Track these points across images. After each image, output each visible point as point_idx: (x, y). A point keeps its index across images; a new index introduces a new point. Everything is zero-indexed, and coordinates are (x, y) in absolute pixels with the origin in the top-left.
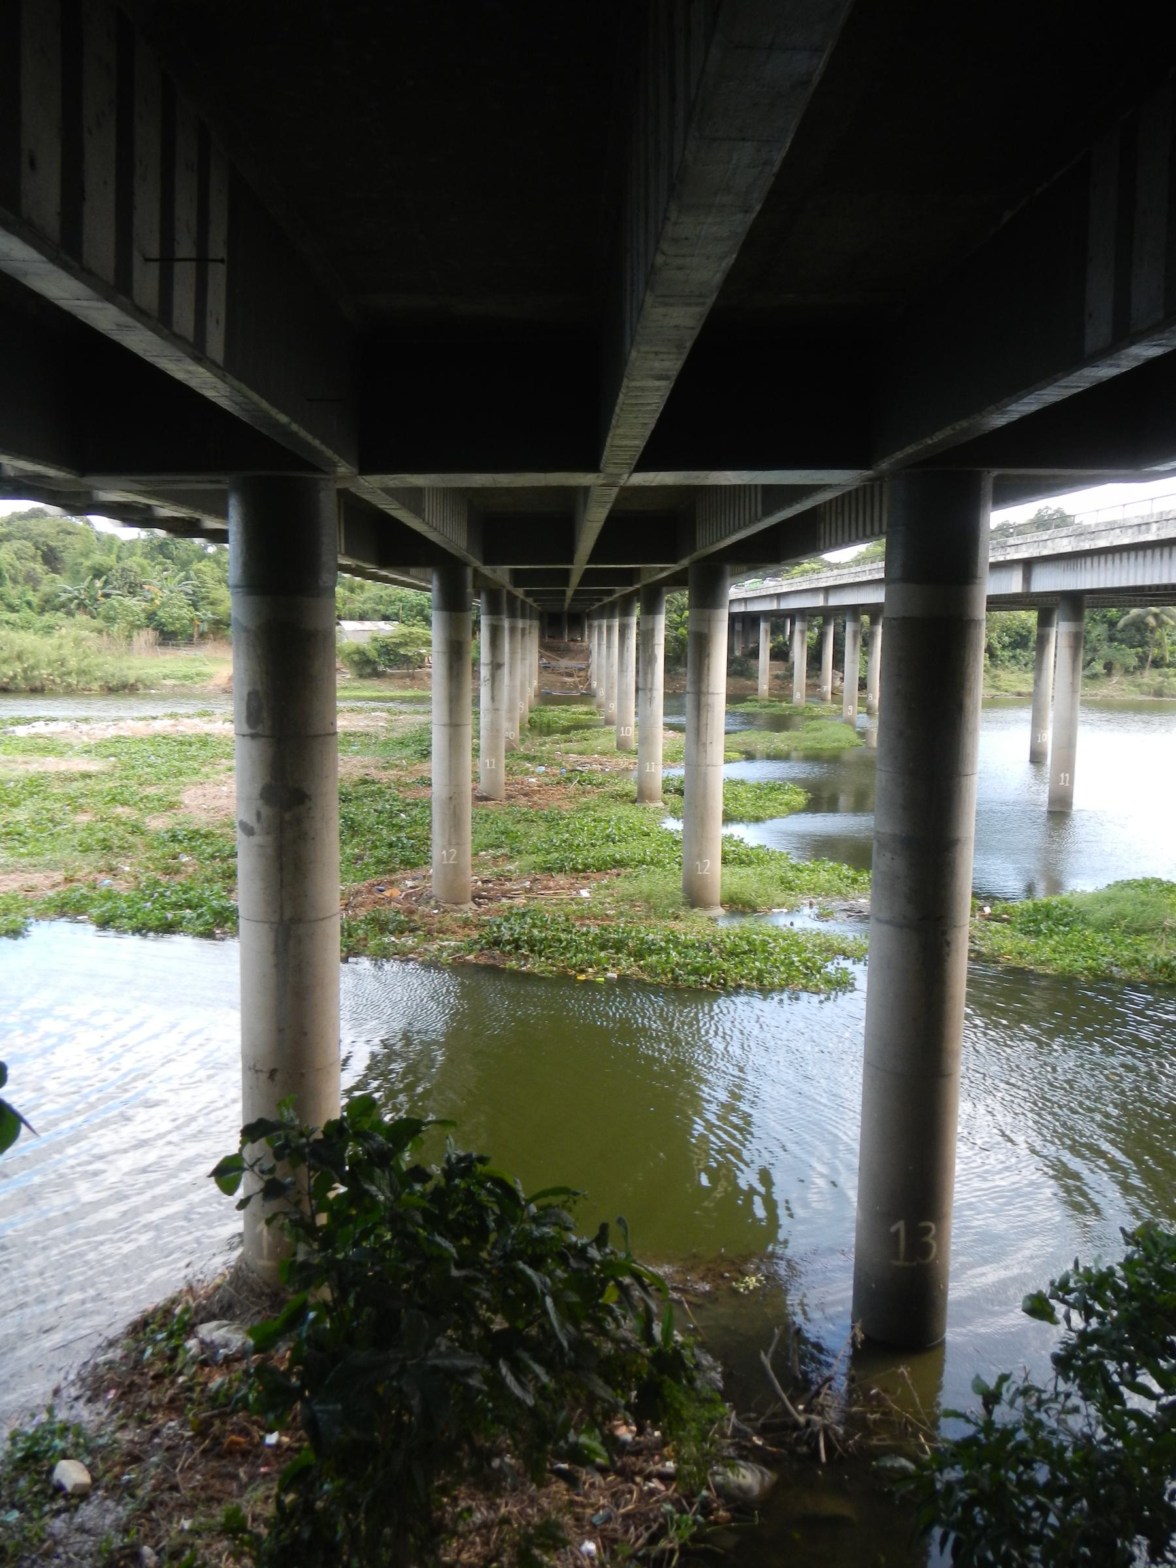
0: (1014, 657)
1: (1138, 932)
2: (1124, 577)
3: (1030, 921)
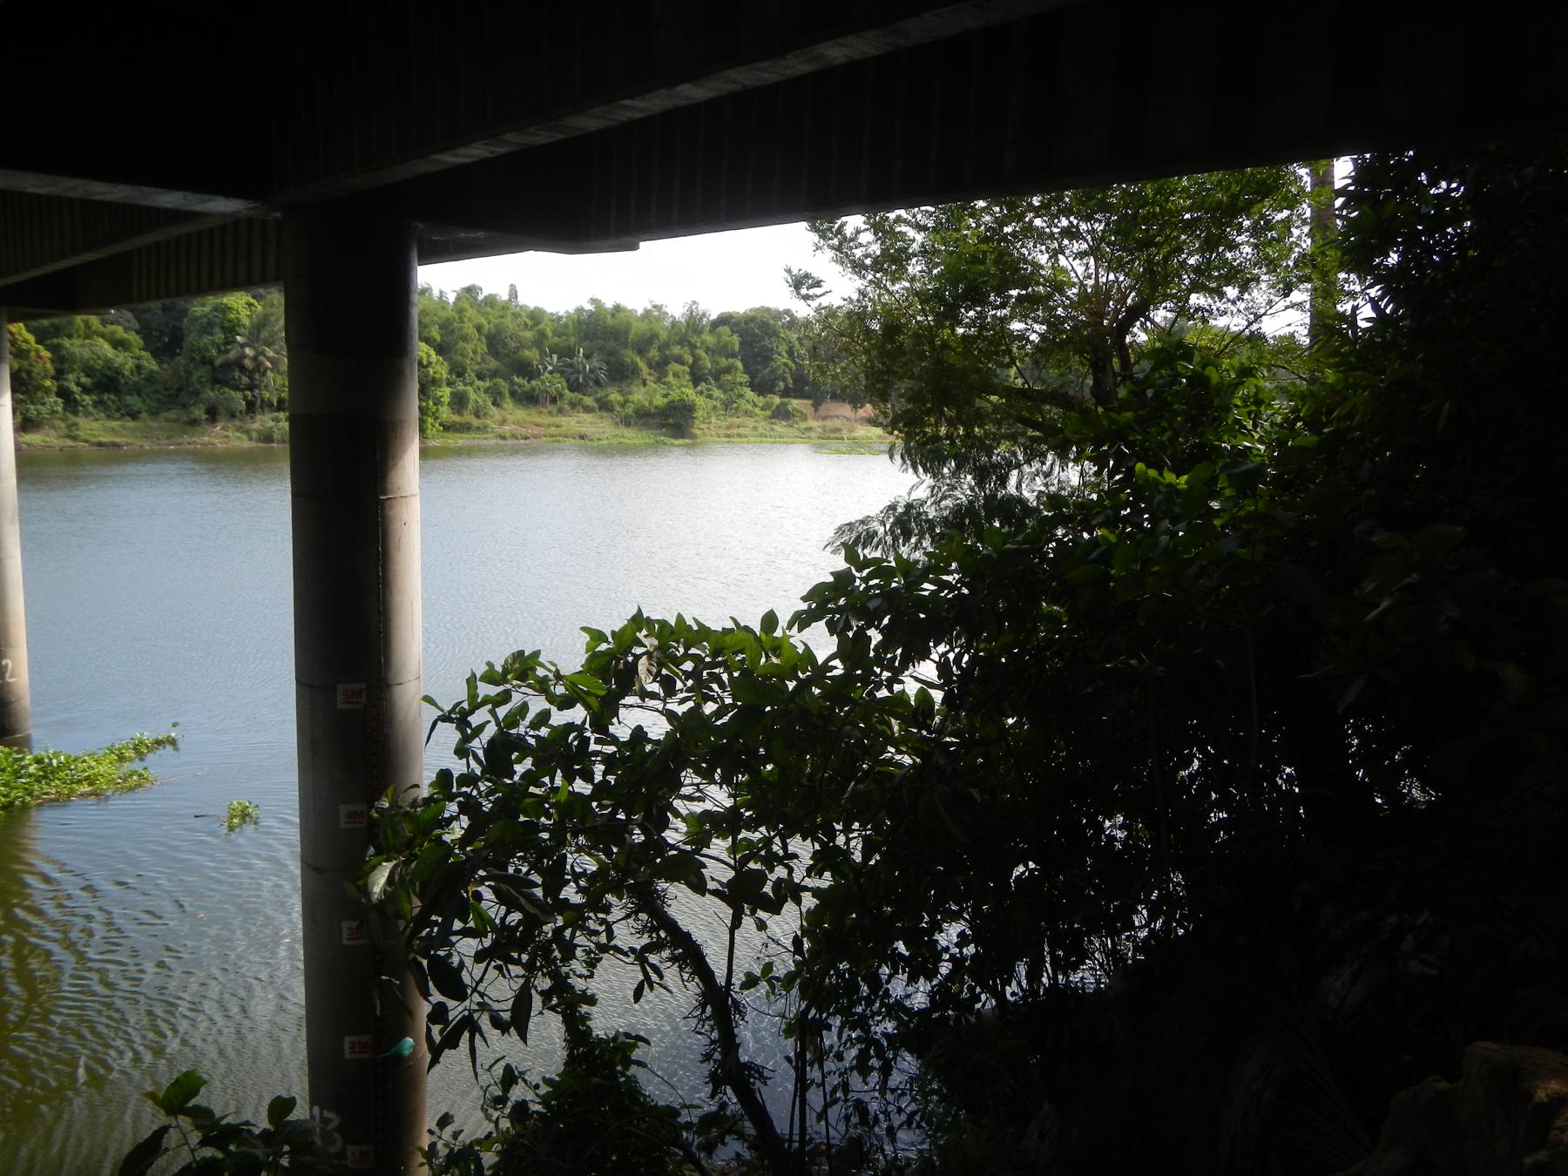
0: (101, 402)
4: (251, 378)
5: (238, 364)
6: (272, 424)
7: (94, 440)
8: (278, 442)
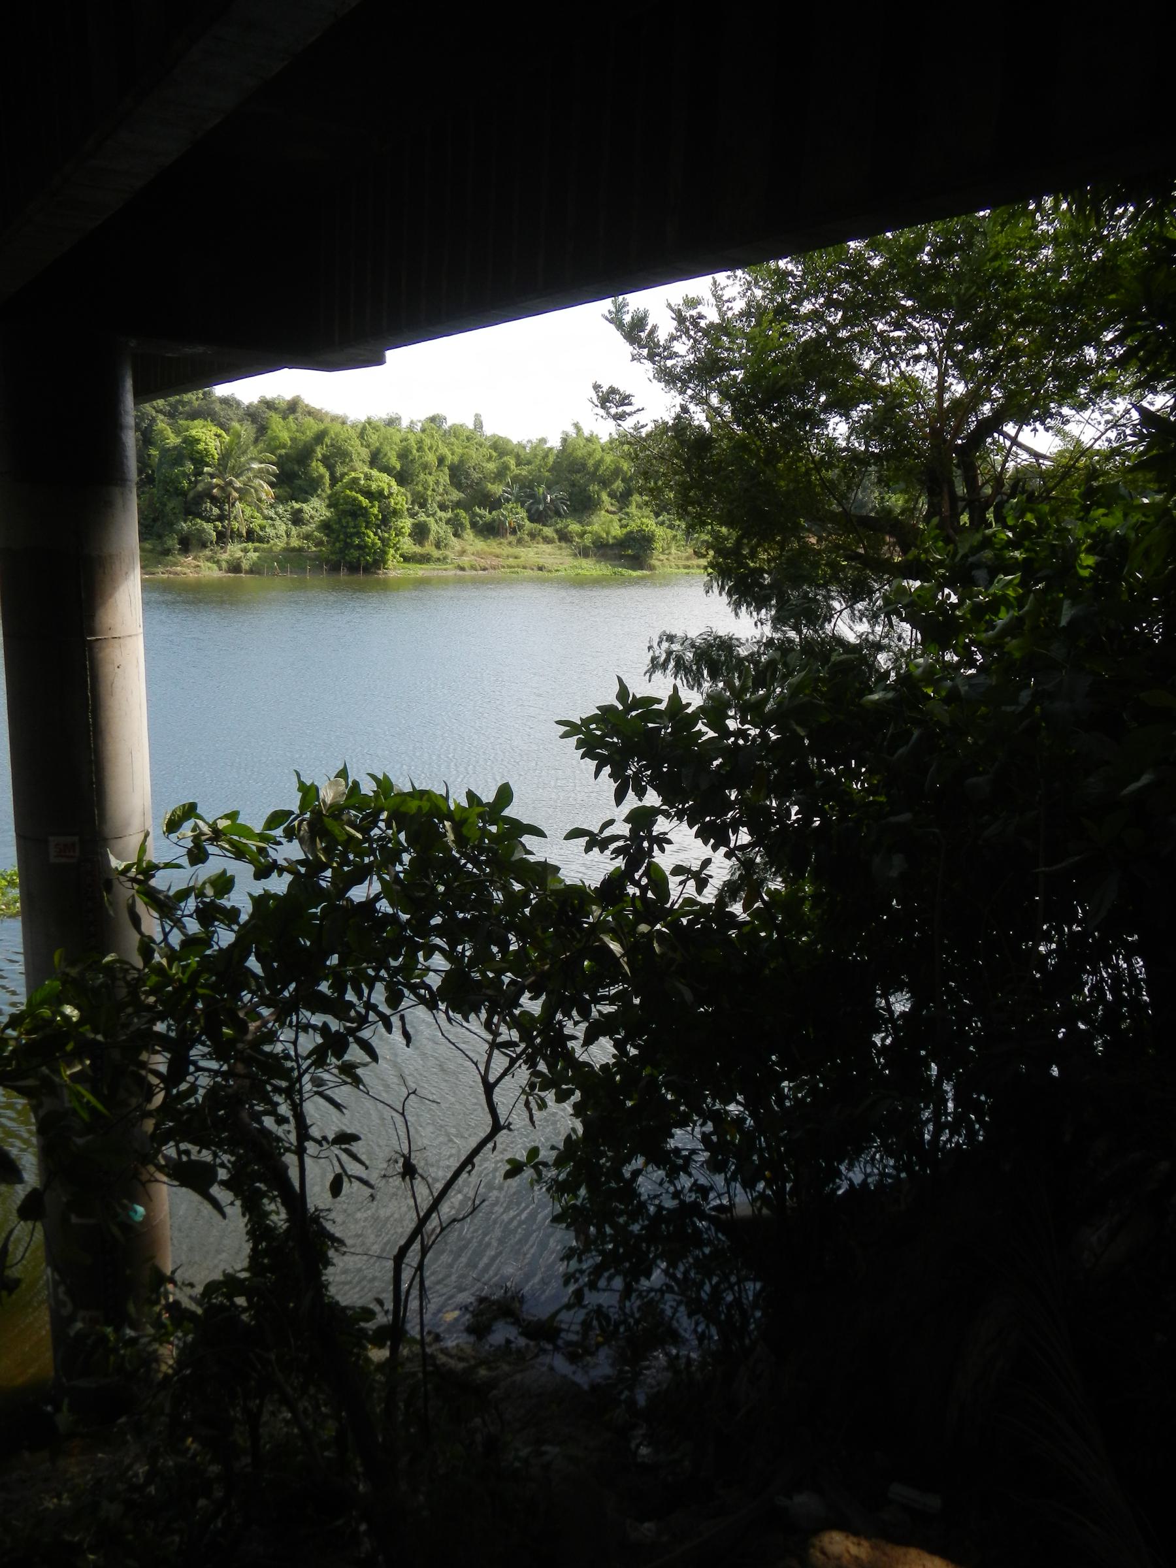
4: (221, 509)
5: (207, 494)
6: (242, 554)
8: (247, 572)
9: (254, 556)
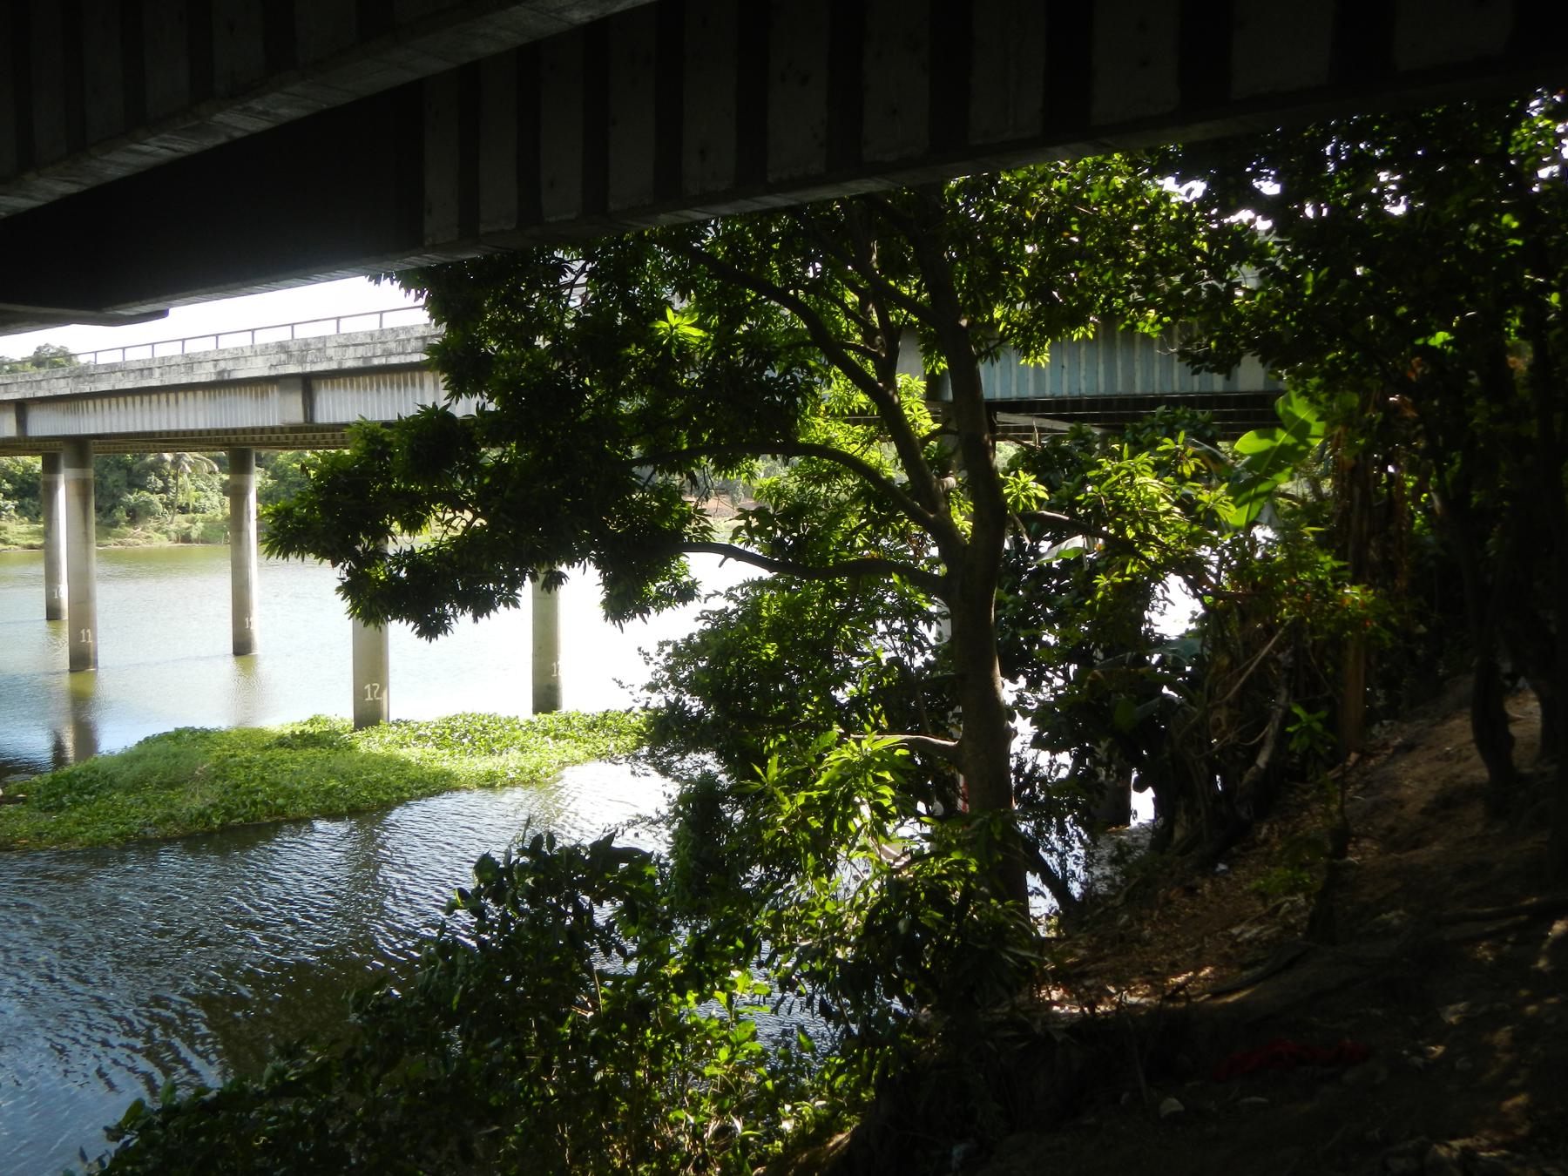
1: (171, 786)
2: (131, 422)
3: (49, 797)
6: (188, 525)
7: (26, 543)
9: (200, 525)
